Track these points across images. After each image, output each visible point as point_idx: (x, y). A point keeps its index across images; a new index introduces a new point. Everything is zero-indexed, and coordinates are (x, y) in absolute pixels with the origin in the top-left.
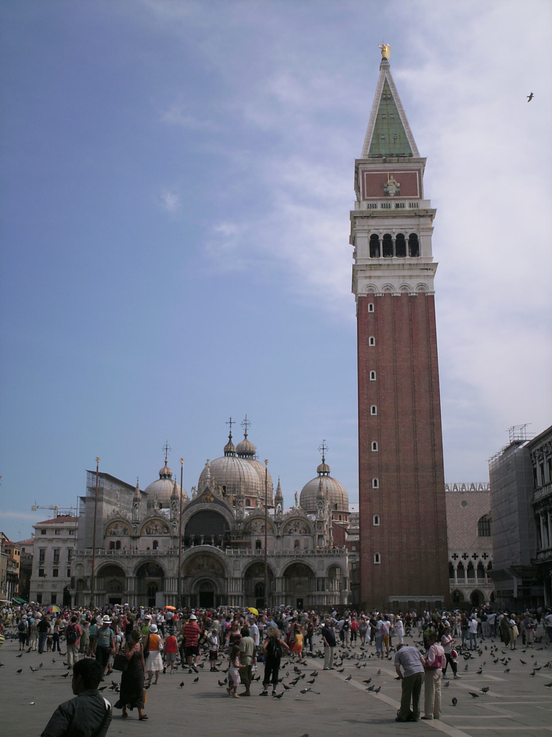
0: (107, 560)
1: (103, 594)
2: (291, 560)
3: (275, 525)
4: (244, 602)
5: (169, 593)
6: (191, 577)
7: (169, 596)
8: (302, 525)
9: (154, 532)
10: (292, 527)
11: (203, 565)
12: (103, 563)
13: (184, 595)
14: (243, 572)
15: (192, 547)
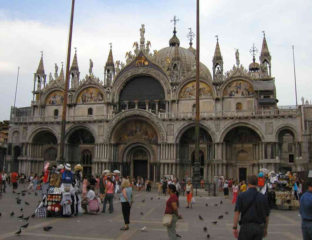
0: (41, 127)
1: (40, 162)
2: (233, 123)
3: (214, 87)
4: (178, 172)
5: (98, 160)
6: (121, 144)
7: (98, 163)
8: (244, 85)
9: (89, 100)
10: (233, 88)
11: (136, 132)
12: (37, 130)
13: (115, 163)
14: (177, 137)
15: (123, 111)
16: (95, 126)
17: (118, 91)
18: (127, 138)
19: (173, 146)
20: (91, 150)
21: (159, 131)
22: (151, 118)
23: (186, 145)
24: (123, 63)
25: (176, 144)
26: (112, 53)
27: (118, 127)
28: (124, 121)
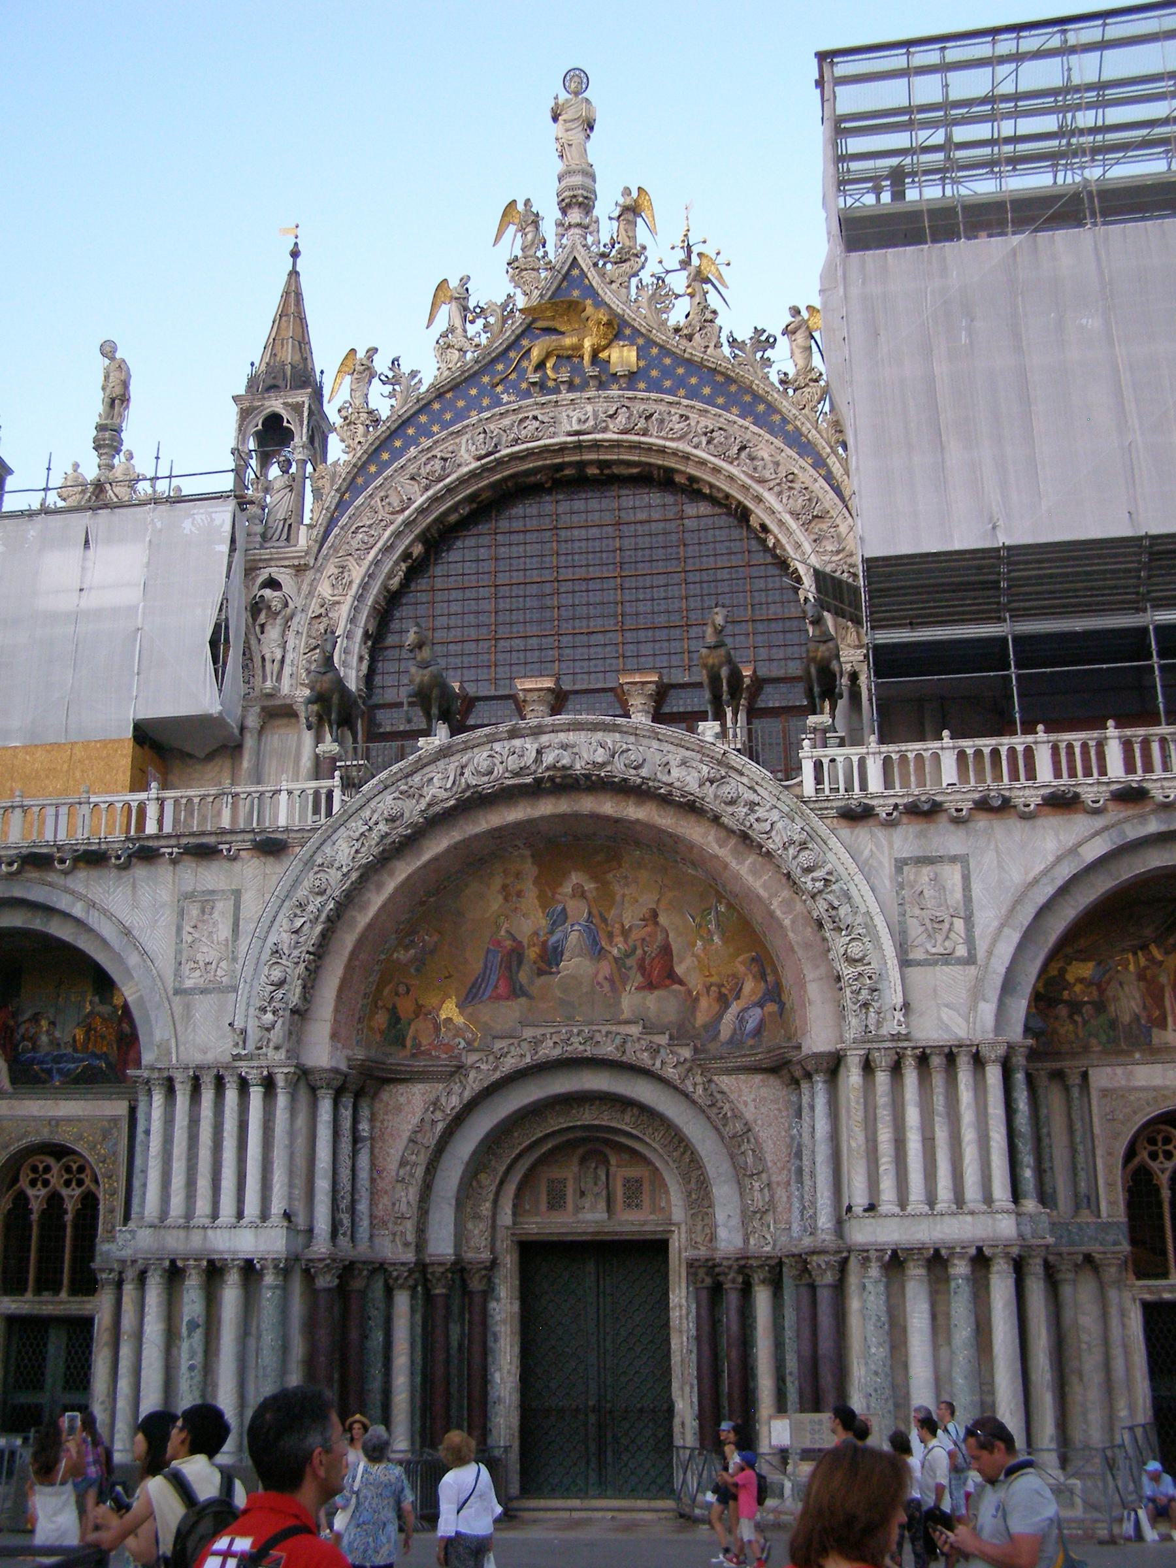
5: (175, 1242)
11: (551, 957)
13: (348, 1270)
16: (146, 894)
17: (360, 598)
18: (459, 1020)
19: (978, 1061)
20: (93, 1148)
21: (820, 925)
22: (732, 802)
23: (1058, 1076)
24: (405, 369)
25: (1001, 1051)
26: (299, 296)
27: (376, 900)
28: (438, 845)
